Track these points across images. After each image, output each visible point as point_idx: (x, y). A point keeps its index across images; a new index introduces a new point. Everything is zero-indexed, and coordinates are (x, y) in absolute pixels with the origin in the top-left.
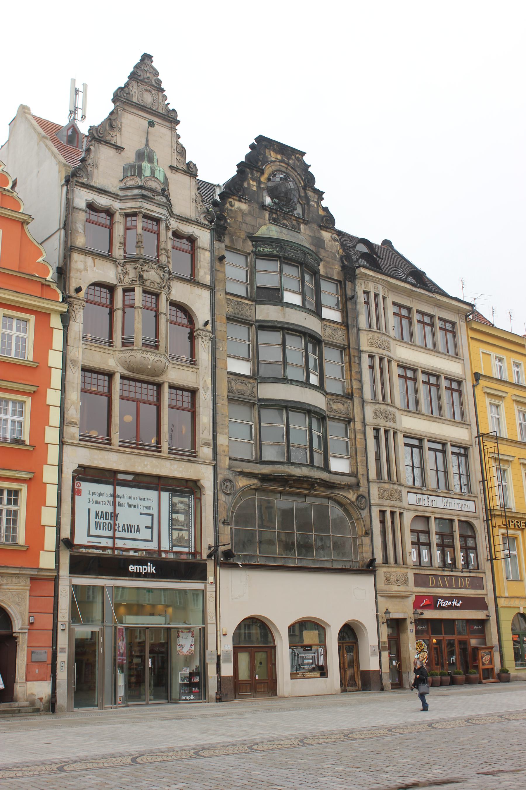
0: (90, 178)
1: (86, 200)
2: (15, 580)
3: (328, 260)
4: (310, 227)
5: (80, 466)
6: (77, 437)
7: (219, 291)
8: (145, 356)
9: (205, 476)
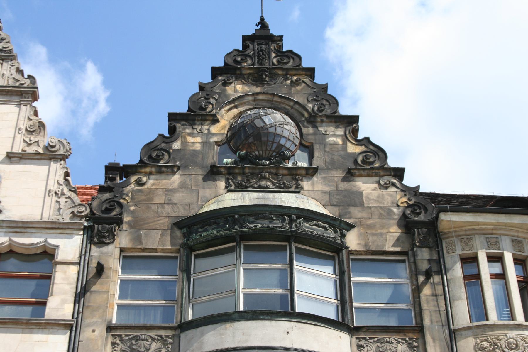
3: (370, 222)
4: (325, 178)
7: (89, 326)
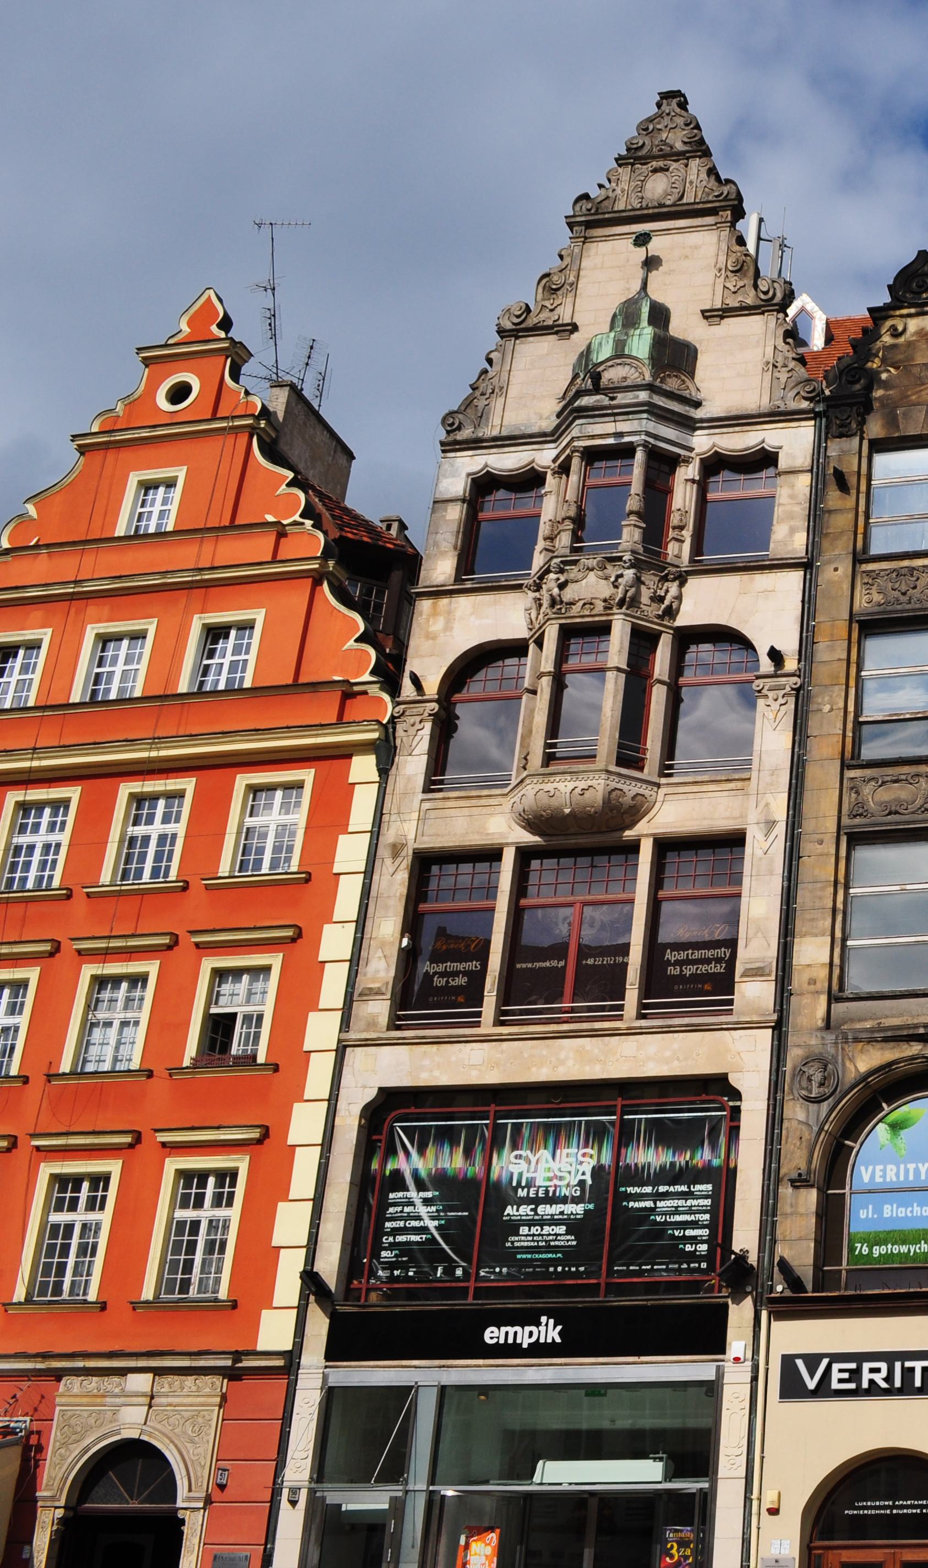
5: (380, 1088)
6: (384, 1020)
7: (829, 562)
8: (549, 787)
9: (745, 1059)
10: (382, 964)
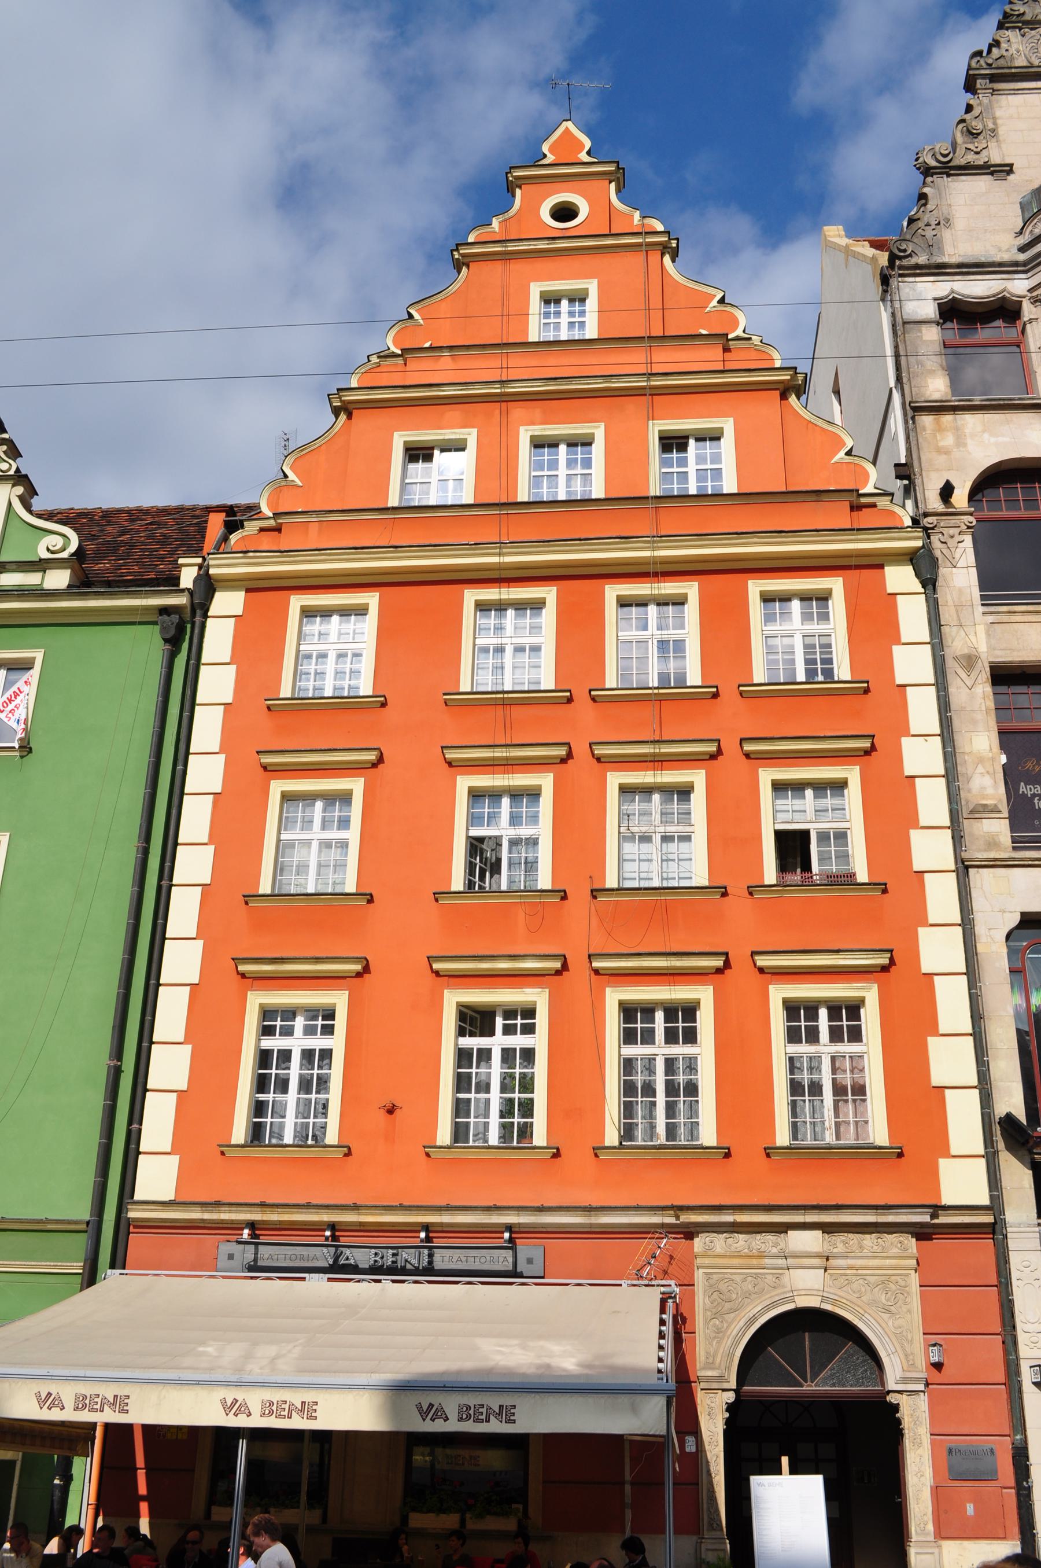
0: (935, 250)
1: (935, 299)
2: (869, 1240)
10: (987, 781)
